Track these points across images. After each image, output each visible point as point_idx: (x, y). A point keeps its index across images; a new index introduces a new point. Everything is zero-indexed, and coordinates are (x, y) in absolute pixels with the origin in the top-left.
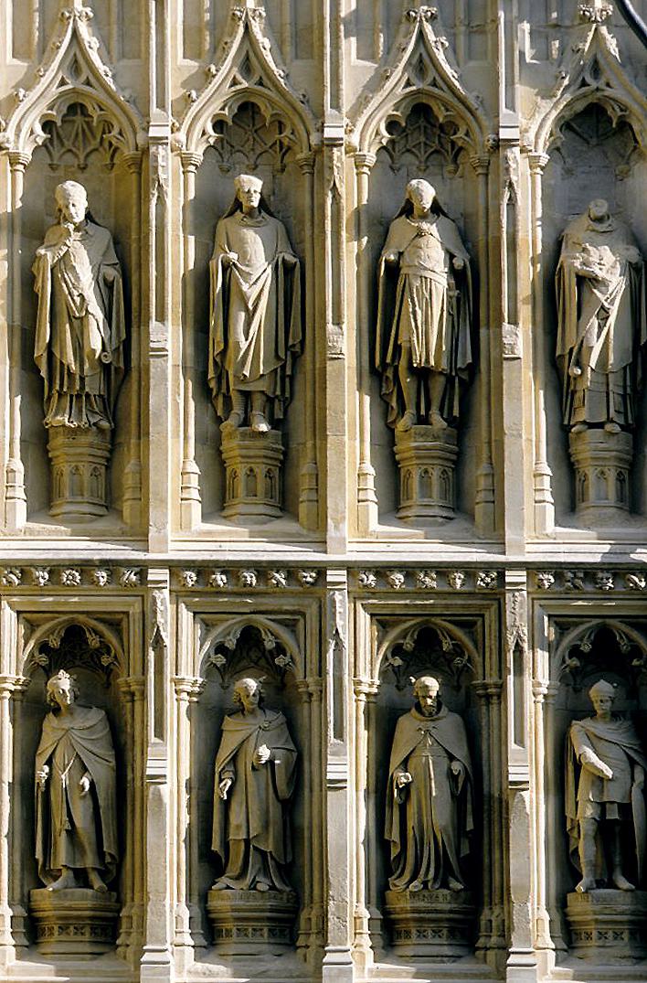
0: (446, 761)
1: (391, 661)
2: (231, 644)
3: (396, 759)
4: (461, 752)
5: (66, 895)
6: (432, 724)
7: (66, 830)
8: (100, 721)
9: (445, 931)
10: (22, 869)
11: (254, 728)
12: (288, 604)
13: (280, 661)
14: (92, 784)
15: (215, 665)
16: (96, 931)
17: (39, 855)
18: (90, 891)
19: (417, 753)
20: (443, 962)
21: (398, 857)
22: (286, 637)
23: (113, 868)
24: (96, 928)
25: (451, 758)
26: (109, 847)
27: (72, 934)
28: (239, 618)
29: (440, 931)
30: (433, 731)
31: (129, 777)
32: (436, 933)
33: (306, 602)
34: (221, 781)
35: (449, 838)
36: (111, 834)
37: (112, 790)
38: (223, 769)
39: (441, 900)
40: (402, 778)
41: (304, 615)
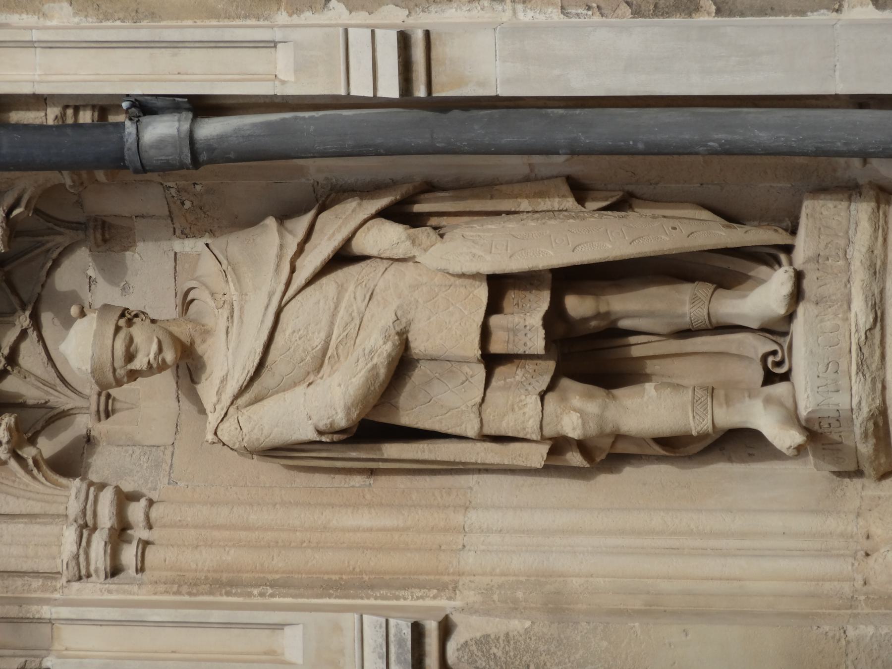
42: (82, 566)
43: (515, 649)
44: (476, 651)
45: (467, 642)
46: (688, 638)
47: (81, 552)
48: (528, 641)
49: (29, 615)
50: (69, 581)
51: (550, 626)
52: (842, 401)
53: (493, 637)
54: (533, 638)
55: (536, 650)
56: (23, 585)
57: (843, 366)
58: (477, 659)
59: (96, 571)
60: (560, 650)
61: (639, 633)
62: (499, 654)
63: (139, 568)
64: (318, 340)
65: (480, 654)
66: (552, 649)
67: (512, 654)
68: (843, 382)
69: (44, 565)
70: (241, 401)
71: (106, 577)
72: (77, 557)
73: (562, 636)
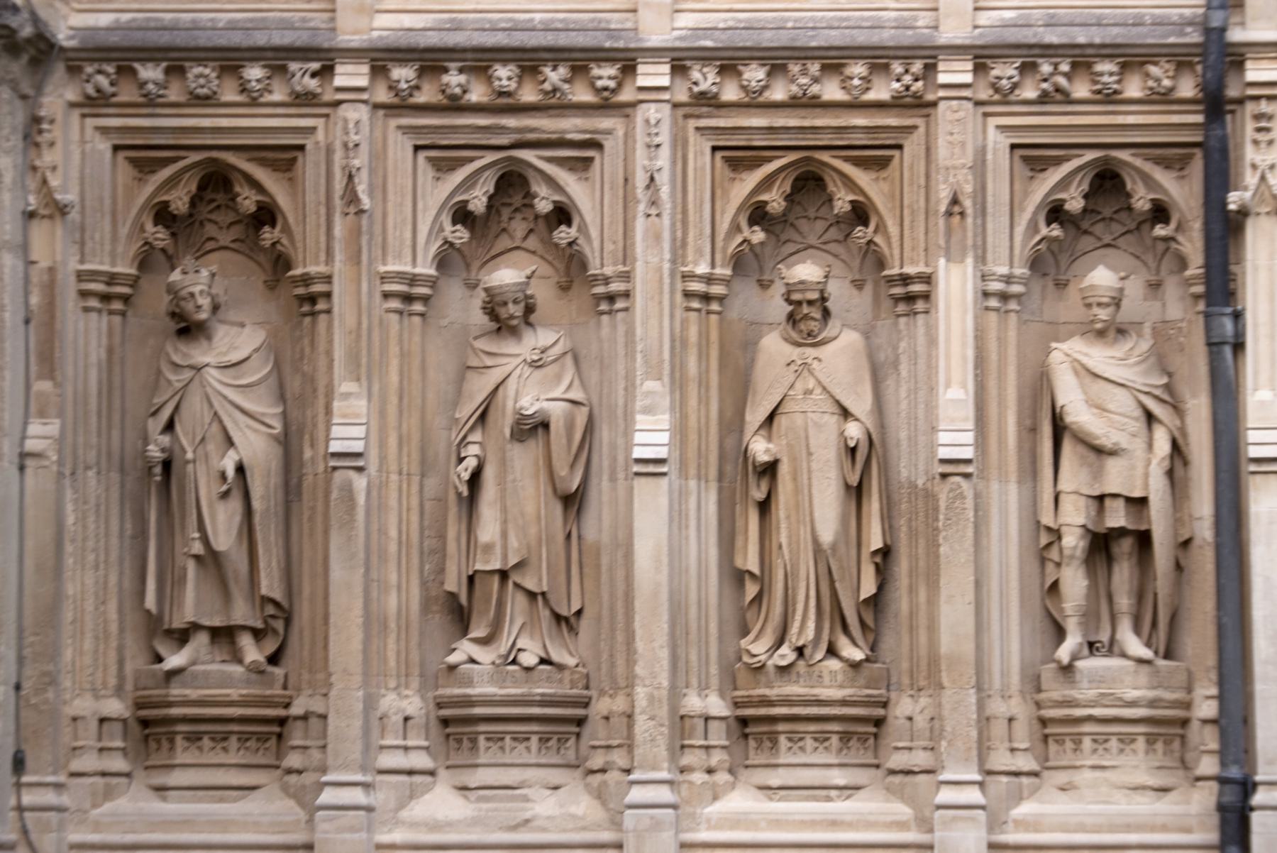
0: (832, 421)
2: (478, 201)
3: (755, 416)
4: (861, 404)
5: (195, 676)
6: (811, 352)
7: (197, 558)
8: (256, 350)
9: (835, 740)
10: (122, 630)
11: (520, 360)
12: (571, 126)
13: (563, 234)
14: (240, 469)
15: (452, 244)
16: (248, 744)
17: (150, 602)
18: (237, 669)
19: (788, 407)
20: (829, 799)
21: (758, 598)
22: (576, 189)
23: (279, 625)
24: (247, 740)
25: (845, 413)
26: (270, 587)
27: (206, 749)
28: (490, 157)
29: (827, 739)
30: (815, 364)
31: (308, 454)
32: (821, 738)
33: (605, 123)
34: (461, 460)
35: (841, 568)
36: (274, 564)
37: (275, 480)
38: (465, 437)
39: (827, 679)
40: (761, 449)
41: (597, 145)
52: (1085, 684)
57: (1103, 685)
64: (1111, 407)
68: (1094, 685)
70: (1079, 367)
72: (993, 274)
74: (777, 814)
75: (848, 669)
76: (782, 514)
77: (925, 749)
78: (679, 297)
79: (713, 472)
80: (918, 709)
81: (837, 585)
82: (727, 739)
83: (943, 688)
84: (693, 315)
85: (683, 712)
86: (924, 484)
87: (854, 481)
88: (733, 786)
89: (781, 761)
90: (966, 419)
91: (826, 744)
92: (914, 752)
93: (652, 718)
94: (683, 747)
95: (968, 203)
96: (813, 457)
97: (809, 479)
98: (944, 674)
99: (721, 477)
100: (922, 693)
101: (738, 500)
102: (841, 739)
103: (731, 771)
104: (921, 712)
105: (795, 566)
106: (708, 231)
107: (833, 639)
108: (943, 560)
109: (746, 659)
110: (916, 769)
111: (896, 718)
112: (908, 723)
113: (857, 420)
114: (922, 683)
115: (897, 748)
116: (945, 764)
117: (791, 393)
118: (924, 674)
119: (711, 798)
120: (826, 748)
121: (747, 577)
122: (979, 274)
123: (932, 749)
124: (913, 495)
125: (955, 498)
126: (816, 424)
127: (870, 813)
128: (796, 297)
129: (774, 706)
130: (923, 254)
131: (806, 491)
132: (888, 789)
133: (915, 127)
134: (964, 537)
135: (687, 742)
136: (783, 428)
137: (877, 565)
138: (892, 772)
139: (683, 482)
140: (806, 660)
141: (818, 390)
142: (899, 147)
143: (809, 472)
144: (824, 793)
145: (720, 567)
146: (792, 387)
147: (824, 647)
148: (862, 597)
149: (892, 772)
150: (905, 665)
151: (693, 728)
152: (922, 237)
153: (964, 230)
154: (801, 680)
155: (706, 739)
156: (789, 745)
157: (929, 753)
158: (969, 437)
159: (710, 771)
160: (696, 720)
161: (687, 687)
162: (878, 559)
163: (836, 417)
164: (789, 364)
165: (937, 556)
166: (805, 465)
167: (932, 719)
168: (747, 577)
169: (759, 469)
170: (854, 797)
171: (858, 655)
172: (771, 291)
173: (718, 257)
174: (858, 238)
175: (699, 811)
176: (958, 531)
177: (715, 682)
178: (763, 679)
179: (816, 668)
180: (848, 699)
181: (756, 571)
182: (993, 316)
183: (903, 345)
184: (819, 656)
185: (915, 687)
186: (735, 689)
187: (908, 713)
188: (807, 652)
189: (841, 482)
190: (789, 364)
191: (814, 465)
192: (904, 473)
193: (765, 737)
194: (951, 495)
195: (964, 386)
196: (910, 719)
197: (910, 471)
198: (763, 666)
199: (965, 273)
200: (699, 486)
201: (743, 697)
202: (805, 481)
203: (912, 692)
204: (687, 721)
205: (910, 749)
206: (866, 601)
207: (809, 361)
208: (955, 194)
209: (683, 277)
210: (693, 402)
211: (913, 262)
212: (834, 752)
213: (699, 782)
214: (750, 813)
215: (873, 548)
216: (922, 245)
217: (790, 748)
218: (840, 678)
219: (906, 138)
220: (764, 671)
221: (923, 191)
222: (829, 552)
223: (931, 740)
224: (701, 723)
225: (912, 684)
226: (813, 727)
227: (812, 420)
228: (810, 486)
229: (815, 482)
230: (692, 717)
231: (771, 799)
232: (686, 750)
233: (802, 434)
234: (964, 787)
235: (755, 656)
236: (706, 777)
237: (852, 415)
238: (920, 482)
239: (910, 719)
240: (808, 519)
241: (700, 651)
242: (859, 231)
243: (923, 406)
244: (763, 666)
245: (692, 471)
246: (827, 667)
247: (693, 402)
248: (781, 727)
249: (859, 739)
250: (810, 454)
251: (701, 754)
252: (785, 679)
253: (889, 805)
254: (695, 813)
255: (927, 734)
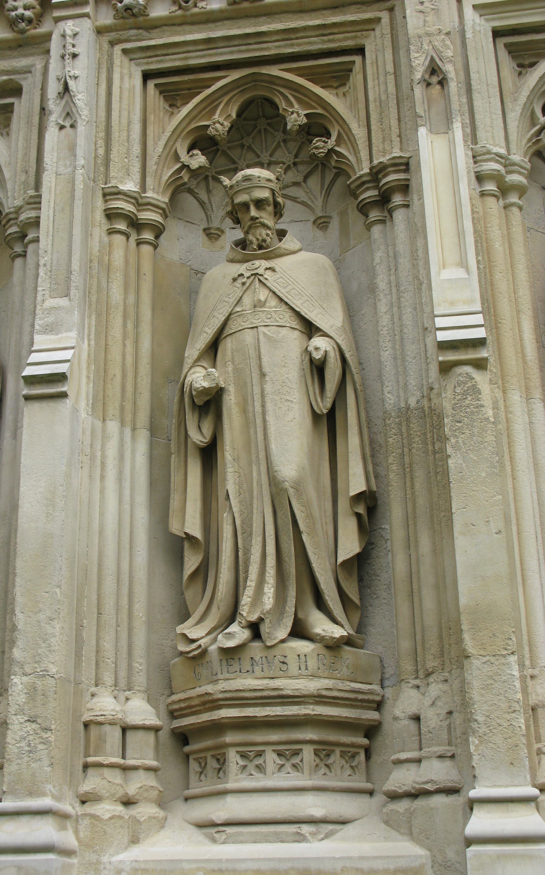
1: (184, 158)
9: (308, 752)
20: (300, 838)
29: (296, 753)
35: (309, 516)
39: (293, 668)
42: (482, 157)
43: (472, 412)
44: (467, 385)
45: (474, 379)
46: (495, 535)
47: (493, 156)
48: (479, 421)
49: (454, 116)
50: (472, 149)
51: (492, 435)
53: (479, 396)
54: (482, 424)
55: (472, 426)
56: (466, 124)
58: (462, 387)
59: (481, 166)
60: (475, 443)
61: (495, 498)
62: (467, 402)
63: (484, 192)
65: (466, 388)
66: (475, 438)
67: (468, 410)
69: (481, 134)
71: (476, 172)
72: (489, 152)
73: (486, 444)
74: (220, 861)
75: (324, 651)
76: (228, 456)
77: (440, 757)
78: (99, 216)
79: (143, 417)
80: (427, 701)
81: (305, 537)
82: (157, 759)
83: (468, 657)
84: (119, 239)
85: (86, 717)
86: (418, 402)
87: (324, 407)
88: (162, 824)
89: (230, 785)
90: (472, 301)
91: (296, 760)
92: (424, 764)
93: (32, 720)
94: (86, 766)
95: (449, 69)
96: (267, 378)
97: (263, 406)
98: (467, 637)
99: (153, 430)
100: (431, 679)
101: (173, 449)
102: (316, 753)
103: (161, 803)
104: (433, 704)
105: (248, 521)
106: (136, 149)
107: (301, 616)
108: (453, 476)
109: (183, 647)
110: (429, 787)
111: (396, 719)
112: (413, 726)
113: (326, 335)
114: (431, 664)
115: (399, 762)
116: (477, 773)
117: (238, 309)
118: (434, 650)
119: (126, 840)
120: (294, 766)
121: (186, 545)
122: (470, 153)
123: (453, 757)
124: (404, 424)
125: (465, 394)
126: (269, 339)
127: (362, 858)
128: (242, 198)
129: (220, 707)
130: (396, 140)
131: (259, 421)
132: (386, 823)
133: (379, 20)
134: (482, 443)
135: (90, 759)
136: (229, 352)
137: (358, 516)
138: (394, 796)
139: (99, 424)
140: (263, 642)
141: (273, 302)
142: (361, 51)
143: (263, 396)
144: (292, 829)
145: (151, 538)
146: (239, 301)
147: (288, 623)
148: (340, 560)
149: (394, 796)
150: (405, 645)
151: (102, 739)
152: (394, 123)
153: (447, 98)
154: (257, 669)
155: (124, 757)
156: (242, 763)
157: (448, 763)
158: (479, 319)
159: (128, 803)
160: (107, 728)
161: (97, 685)
162: (361, 509)
163: (297, 333)
164: (235, 280)
165: (446, 473)
166: (257, 390)
167: (450, 713)
168: (186, 545)
169: (199, 402)
170: (338, 835)
171: (337, 632)
172: (220, 242)
173: (149, 181)
174: (316, 148)
175: (105, 859)
176: (472, 435)
177: (140, 679)
178: (204, 672)
179: (277, 651)
180: (324, 693)
181: (196, 532)
182: (491, 202)
183: (379, 255)
184: (283, 633)
185: (421, 674)
186: (172, 693)
187: (413, 710)
188: (264, 629)
189: (307, 408)
190: (235, 280)
191: (268, 388)
192: (390, 400)
193: (209, 755)
194: (458, 390)
195: (463, 264)
196: (417, 719)
197: (398, 397)
198: (204, 652)
199: (452, 143)
200: (122, 433)
201: (180, 701)
202: (258, 408)
203: (417, 682)
204: (94, 730)
205: (419, 761)
206: (344, 563)
207: (260, 271)
208: (432, 59)
209: (104, 195)
210: (116, 331)
211: (384, 153)
212: (306, 771)
213: (107, 816)
214: (181, 861)
215: (353, 492)
216: (395, 130)
217: (245, 767)
218: (312, 663)
219: (367, 37)
220: (207, 659)
221: (391, 79)
222: (291, 492)
223: (450, 744)
224: (118, 733)
225: (417, 671)
226: (274, 737)
227: (265, 334)
228: (264, 413)
229: (269, 406)
230: (101, 724)
231: (214, 841)
232: (90, 771)
233: (253, 353)
234: (511, 806)
235: (193, 641)
236: (120, 809)
237: (318, 330)
238: (412, 402)
239: (417, 719)
240: (262, 455)
241: (117, 639)
242: (317, 142)
243: (409, 310)
244: (204, 652)
245: (113, 409)
246: (292, 648)
247: (116, 331)
248: (229, 738)
249: (343, 754)
250: (263, 375)
251: (116, 777)
252: (236, 667)
253: (389, 844)
254: (99, 862)
255: (445, 736)
